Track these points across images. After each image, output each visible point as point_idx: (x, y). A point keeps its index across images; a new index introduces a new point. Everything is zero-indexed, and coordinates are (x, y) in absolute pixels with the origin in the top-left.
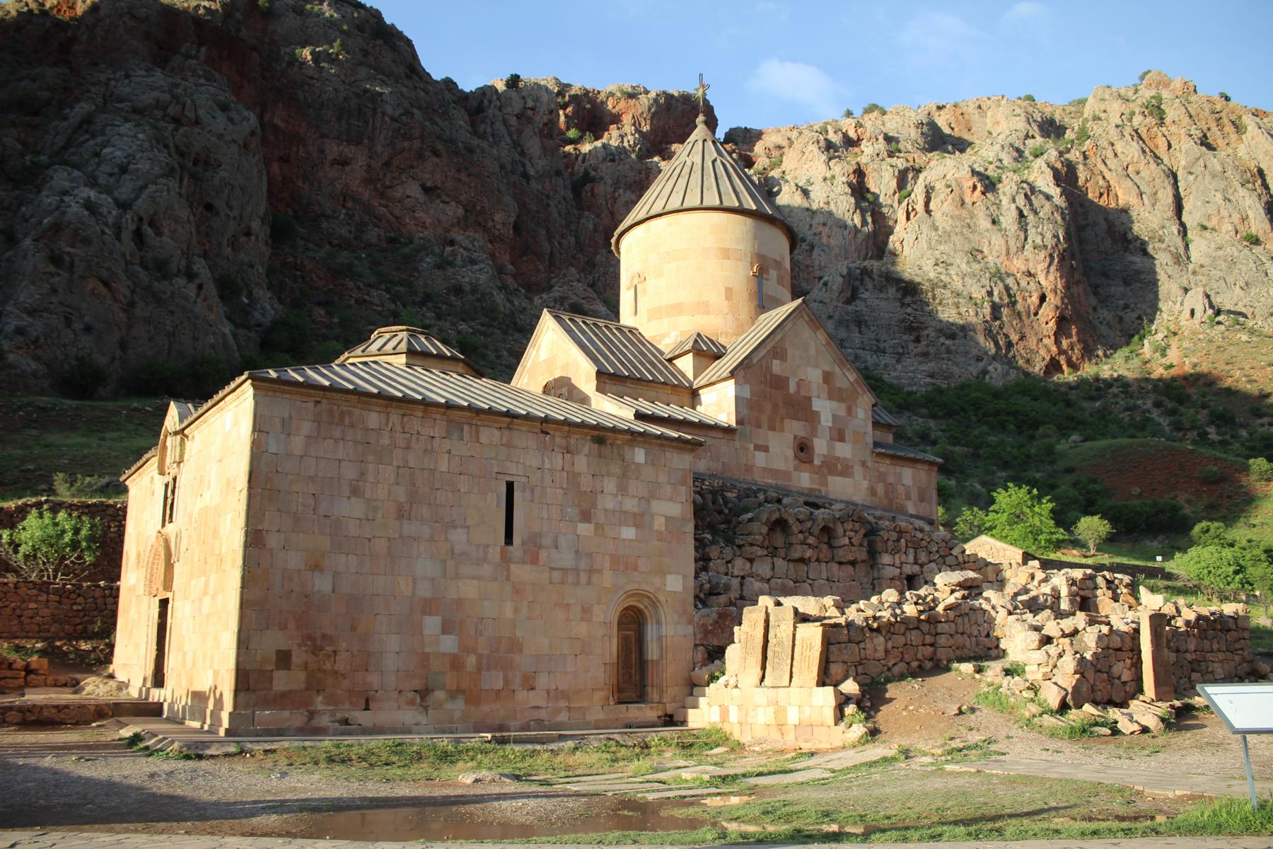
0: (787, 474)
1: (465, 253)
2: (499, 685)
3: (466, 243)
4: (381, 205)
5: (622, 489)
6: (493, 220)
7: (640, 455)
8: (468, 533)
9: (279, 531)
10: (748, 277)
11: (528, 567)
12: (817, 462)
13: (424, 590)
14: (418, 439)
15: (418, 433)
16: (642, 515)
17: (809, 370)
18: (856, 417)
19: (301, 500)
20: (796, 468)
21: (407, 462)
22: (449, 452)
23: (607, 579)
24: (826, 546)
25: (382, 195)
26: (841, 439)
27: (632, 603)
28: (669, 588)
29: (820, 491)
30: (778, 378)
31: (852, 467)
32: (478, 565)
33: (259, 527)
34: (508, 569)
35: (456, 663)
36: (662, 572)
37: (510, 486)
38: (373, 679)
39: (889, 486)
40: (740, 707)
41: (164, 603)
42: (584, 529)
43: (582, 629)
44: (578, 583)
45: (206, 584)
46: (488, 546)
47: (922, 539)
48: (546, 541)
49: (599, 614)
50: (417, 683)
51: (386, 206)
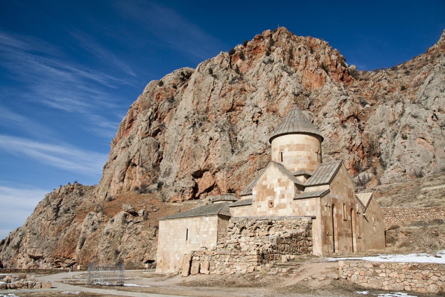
0: (266, 212)
5: (204, 227)
10: (278, 155)
12: (275, 206)
13: (176, 250)
16: (207, 232)
18: (289, 189)
20: (269, 210)
26: (283, 196)
29: (275, 215)
30: (265, 186)
31: (286, 205)
36: (211, 243)
37: (187, 229)
38: (170, 264)
39: (299, 208)
42: (198, 236)
48: (192, 239)
50: (175, 265)
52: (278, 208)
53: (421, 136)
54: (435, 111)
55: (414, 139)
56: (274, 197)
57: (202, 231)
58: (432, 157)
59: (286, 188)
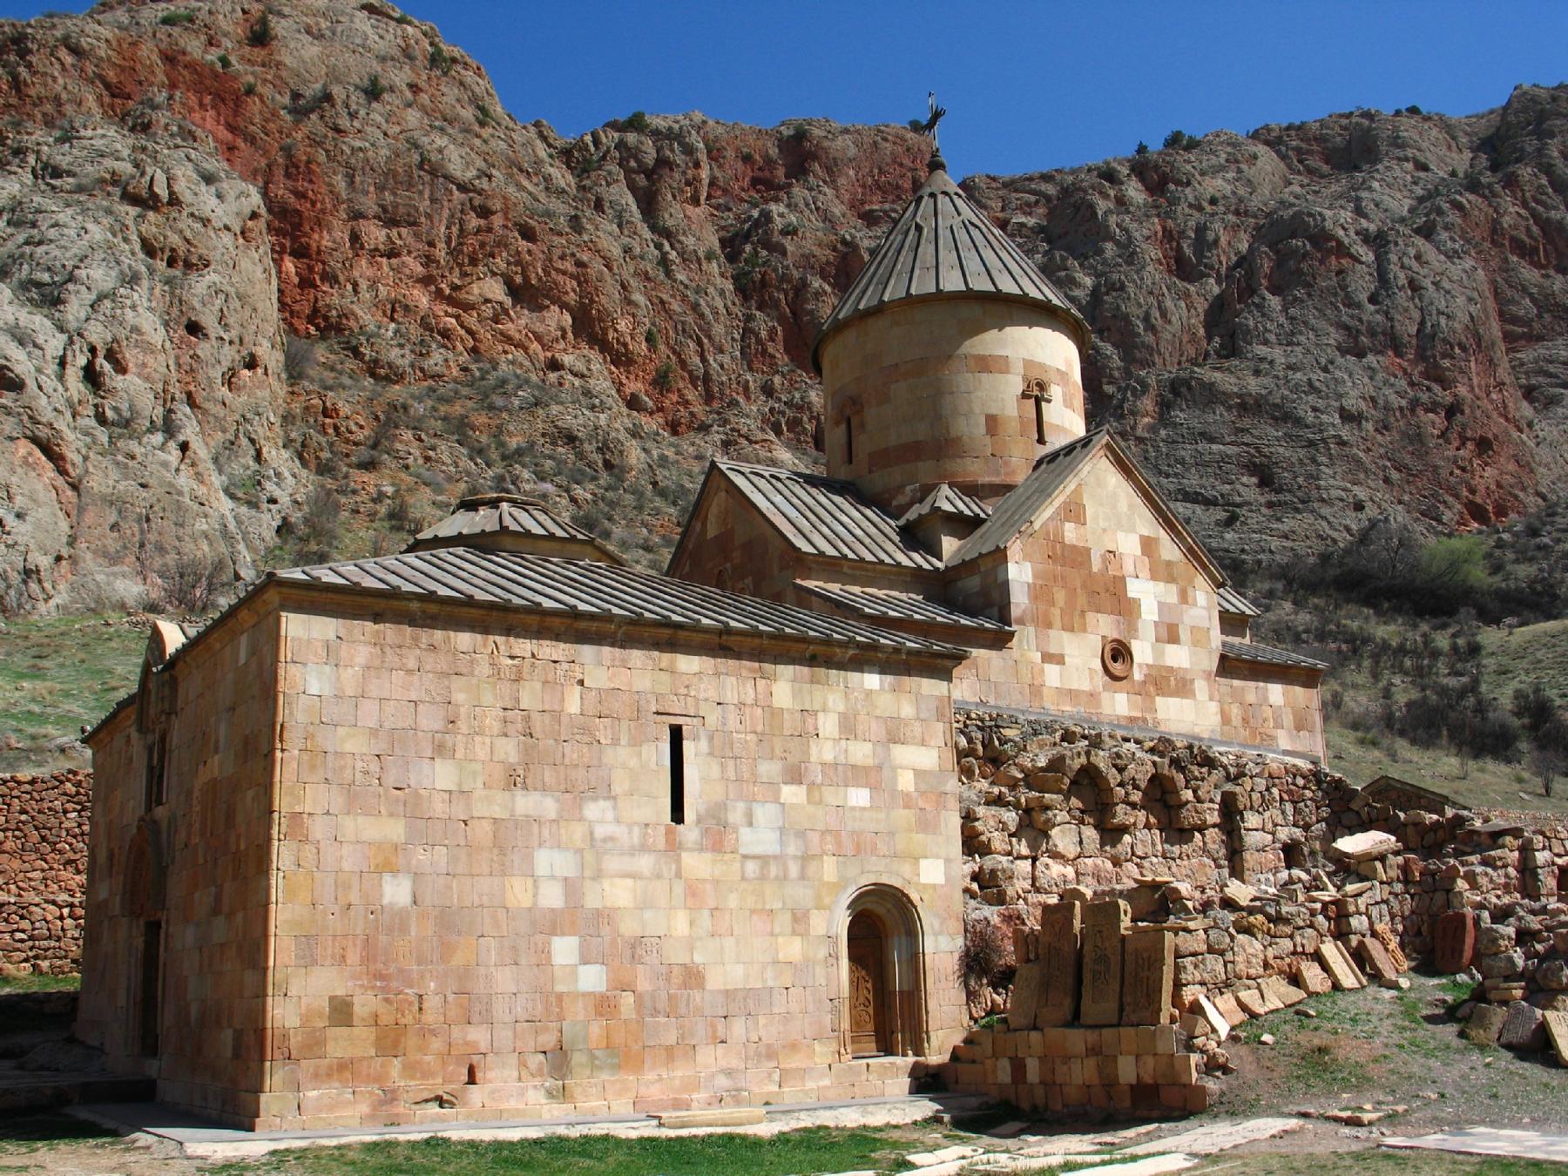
1: (577, 382)
2: (671, 1038)
3: (580, 366)
4: (447, 314)
5: (849, 728)
6: (616, 330)
7: (872, 680)
8: (615, 808)
9: (328, 813)
11: (708, 856)
12: (1138, 675)
13: (552, 897)
14: (533, 665)
15: (533, 656)
16: (879, 768)
17: (1121, 536)
19: (359, 765)
21: (518, 700)
22: (581, 683)
23: (829, 869)
24: (1158, 805)
25: (451, 301)
27: (869, 906)
28: (924, 879)
29: (1145, 720)
32: (633, 855)
33: (298, 809)
34: (678, 861)
35: (603, 1005)
38: (478, 1035)
40: (1043, 1059)
41: (153, 928)
42: (792, 794)
43: (793, 949)
44: (785, 878)
45: (218, 898)
46: (647, 825)
47: (1304, 788)
48: (736, 815)
49: (818, 923)
51: (457, 317)
52: (1152, 689)
53: (43, 432)
54: (93, 350)
55: (11, 439)
56: (1132, 629)
57: (828, 756)
58: (64, 540)
59: (1184, 597)
